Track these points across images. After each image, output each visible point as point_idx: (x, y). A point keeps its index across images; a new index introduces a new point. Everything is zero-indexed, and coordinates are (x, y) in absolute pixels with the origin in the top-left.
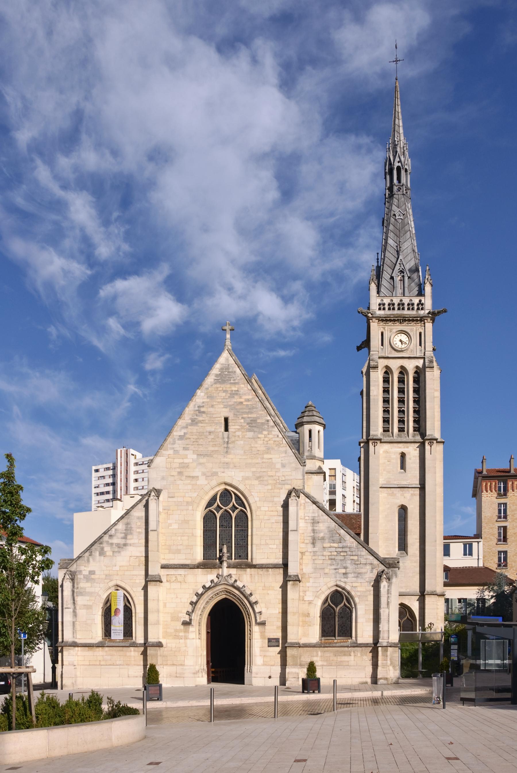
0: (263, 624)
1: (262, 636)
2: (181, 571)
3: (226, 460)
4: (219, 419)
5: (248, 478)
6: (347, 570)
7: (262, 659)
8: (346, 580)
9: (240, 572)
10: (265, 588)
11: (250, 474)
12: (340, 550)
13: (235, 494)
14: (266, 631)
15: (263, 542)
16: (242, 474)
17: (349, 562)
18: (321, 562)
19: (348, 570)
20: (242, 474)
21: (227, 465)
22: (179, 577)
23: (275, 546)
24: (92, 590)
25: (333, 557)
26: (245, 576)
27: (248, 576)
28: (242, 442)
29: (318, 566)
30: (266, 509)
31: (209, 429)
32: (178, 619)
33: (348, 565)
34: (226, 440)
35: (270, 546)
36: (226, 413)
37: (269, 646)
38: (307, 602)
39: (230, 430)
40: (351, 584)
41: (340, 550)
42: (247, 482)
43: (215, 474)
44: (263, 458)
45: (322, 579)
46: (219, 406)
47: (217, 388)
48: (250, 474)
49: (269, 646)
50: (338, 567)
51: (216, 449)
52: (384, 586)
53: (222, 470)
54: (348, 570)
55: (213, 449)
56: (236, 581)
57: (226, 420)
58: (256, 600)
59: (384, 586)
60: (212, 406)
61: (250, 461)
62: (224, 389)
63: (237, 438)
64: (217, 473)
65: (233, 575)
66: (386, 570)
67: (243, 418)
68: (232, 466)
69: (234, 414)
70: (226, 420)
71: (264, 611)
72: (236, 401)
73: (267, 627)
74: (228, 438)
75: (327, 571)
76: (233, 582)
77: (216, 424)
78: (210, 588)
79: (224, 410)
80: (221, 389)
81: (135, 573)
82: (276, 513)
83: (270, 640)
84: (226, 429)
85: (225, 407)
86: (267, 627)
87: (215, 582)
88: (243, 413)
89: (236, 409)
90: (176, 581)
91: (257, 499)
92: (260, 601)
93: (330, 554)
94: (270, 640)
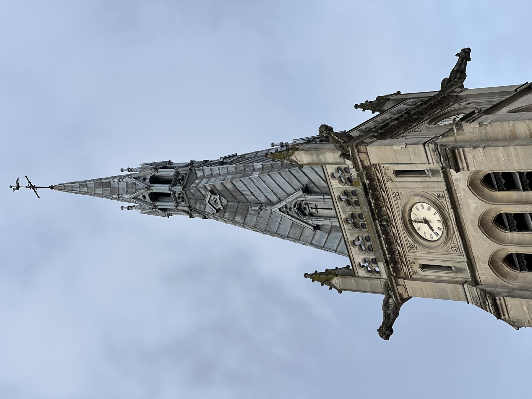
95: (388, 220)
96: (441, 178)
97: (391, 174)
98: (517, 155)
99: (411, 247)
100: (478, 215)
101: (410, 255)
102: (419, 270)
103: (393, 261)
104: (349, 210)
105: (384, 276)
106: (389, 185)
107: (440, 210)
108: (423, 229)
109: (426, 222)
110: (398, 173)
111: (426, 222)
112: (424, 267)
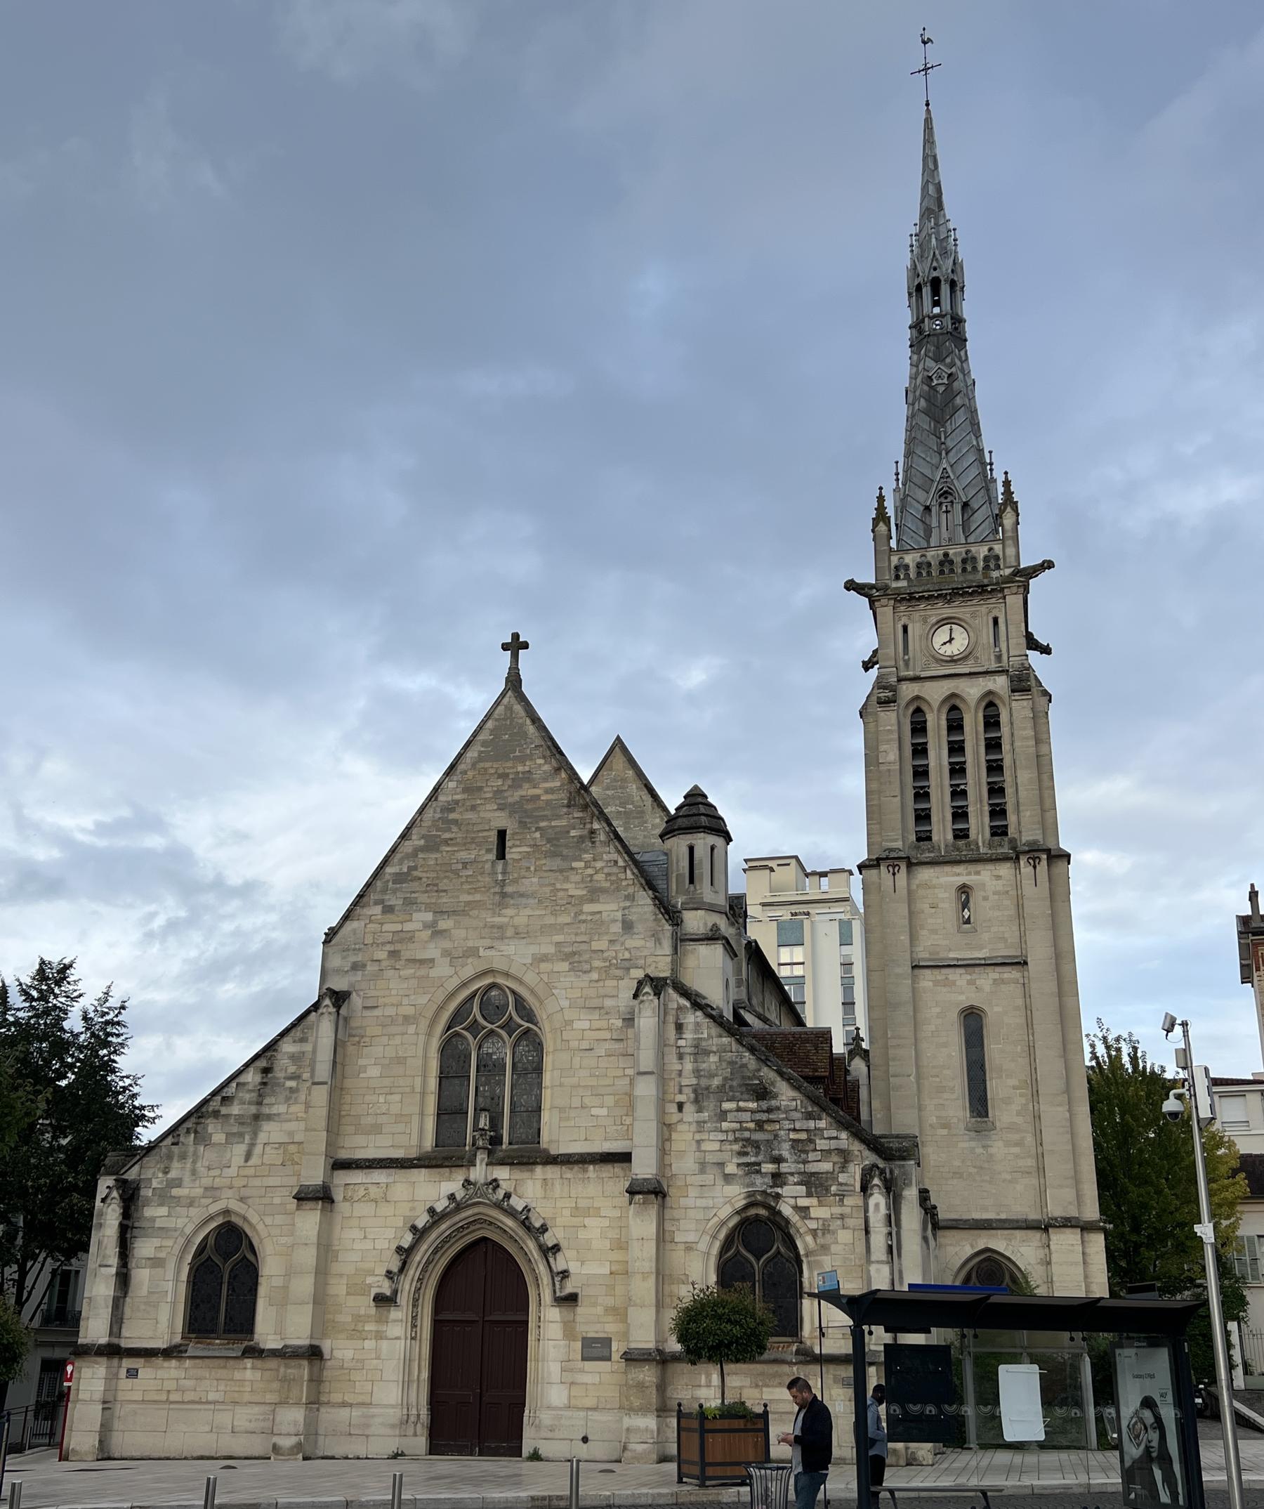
0: (572, 1299)
1: (569, 1331)
2: (379, 1176)
3: (497, 920)
4: (485, 834)
5: (544, 958)
6: (783, 1165)
7: (566, 1392)
8: (779, 1190)
9: (519, 1174)
10: (577, 1211)
11: (552, 950)
12: (764, 1117)
13: (513, 992)
14: (578, 1319)
15: (576, 1102)
16: (534, 949)
17: (786, 1146)
18: (716, 1146)
19: (784, 1167)
20: (534, 949)
21: (500, 932)
22: (374, 1191)
23: (604, 1112)
24: (170, 1223)
25: (747, 1134)
26: (530, 1182)
27: (539, 1184)
28: (535, 880)
29: (710, 1158)
30: (586, 1025)
31: (463, 855)
32: (362, 1290)
33: (786, 1154)
34: (500, 877)
35: (594, 1111)
36: (502, 820)
37: (583, 1359)
38: (682, 1247)
39: (507, 856)
40: (792, 1201)
41: (764, 1117)
42: (543, 966)
43: (473, 952)
44: (581, 912)
45: (718, 1188)
46: (488, 807)
47: (486, 769)
48: (552, 950)
49: (583, 1359)
50: (760, 1158)
51: (478, 897)
52: (877, 1205)
53: (488, 942)
54: (784, 1167)
55: (470, 898)
56: (508, 1196)
57: (502, 834)
58: (555, 1242)
59: (877, 1205)
60: (473, 808)
61: (550, 920)
62: (501, 771)
63: (523, 873)
64: (478, 949)
65: (501, 1183)
66: (881, 1164)
67: (538, 829)
68: (510, 932)
69: (520, 822)
70: (502, 834)
71: (573, 1267)
72: (524, 793)
73: (582, 1310)
74: (504, 873)
75: (731, 1169)
76: (501, 1197)
77: (480, 845)
78: (444, 1216)
79: (498, 814)
80: (492, 771)
81: (271, 1181)
82: (607, 1035)
83: (588, 1343)
84: (501, 855)
85: (501, 808)
86: (579, 1310)
87: (458, 1197)
88: (544, 818)
89: (526, 811)
90: (367, 1198)
91: (565, 1003)
92: (563, 1244)
93: (737, 1126)
94: (588, 1343)
95: (949, 602)
96: (993, 666)
97: (995, 613)
98: (1028, 747)
99: (925, 621)
100: (963, 695)
101: (916, 615)
102: (902, 623)
103: (910, 598)
104: (958, 560)
105: (894, 585)
106: (984, 609)
107: (963, 658)
108: (942, 635)
109: (951, 640)
110: (996, 621)
111: (951, 640)
112: (905, 629)
